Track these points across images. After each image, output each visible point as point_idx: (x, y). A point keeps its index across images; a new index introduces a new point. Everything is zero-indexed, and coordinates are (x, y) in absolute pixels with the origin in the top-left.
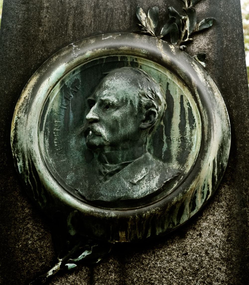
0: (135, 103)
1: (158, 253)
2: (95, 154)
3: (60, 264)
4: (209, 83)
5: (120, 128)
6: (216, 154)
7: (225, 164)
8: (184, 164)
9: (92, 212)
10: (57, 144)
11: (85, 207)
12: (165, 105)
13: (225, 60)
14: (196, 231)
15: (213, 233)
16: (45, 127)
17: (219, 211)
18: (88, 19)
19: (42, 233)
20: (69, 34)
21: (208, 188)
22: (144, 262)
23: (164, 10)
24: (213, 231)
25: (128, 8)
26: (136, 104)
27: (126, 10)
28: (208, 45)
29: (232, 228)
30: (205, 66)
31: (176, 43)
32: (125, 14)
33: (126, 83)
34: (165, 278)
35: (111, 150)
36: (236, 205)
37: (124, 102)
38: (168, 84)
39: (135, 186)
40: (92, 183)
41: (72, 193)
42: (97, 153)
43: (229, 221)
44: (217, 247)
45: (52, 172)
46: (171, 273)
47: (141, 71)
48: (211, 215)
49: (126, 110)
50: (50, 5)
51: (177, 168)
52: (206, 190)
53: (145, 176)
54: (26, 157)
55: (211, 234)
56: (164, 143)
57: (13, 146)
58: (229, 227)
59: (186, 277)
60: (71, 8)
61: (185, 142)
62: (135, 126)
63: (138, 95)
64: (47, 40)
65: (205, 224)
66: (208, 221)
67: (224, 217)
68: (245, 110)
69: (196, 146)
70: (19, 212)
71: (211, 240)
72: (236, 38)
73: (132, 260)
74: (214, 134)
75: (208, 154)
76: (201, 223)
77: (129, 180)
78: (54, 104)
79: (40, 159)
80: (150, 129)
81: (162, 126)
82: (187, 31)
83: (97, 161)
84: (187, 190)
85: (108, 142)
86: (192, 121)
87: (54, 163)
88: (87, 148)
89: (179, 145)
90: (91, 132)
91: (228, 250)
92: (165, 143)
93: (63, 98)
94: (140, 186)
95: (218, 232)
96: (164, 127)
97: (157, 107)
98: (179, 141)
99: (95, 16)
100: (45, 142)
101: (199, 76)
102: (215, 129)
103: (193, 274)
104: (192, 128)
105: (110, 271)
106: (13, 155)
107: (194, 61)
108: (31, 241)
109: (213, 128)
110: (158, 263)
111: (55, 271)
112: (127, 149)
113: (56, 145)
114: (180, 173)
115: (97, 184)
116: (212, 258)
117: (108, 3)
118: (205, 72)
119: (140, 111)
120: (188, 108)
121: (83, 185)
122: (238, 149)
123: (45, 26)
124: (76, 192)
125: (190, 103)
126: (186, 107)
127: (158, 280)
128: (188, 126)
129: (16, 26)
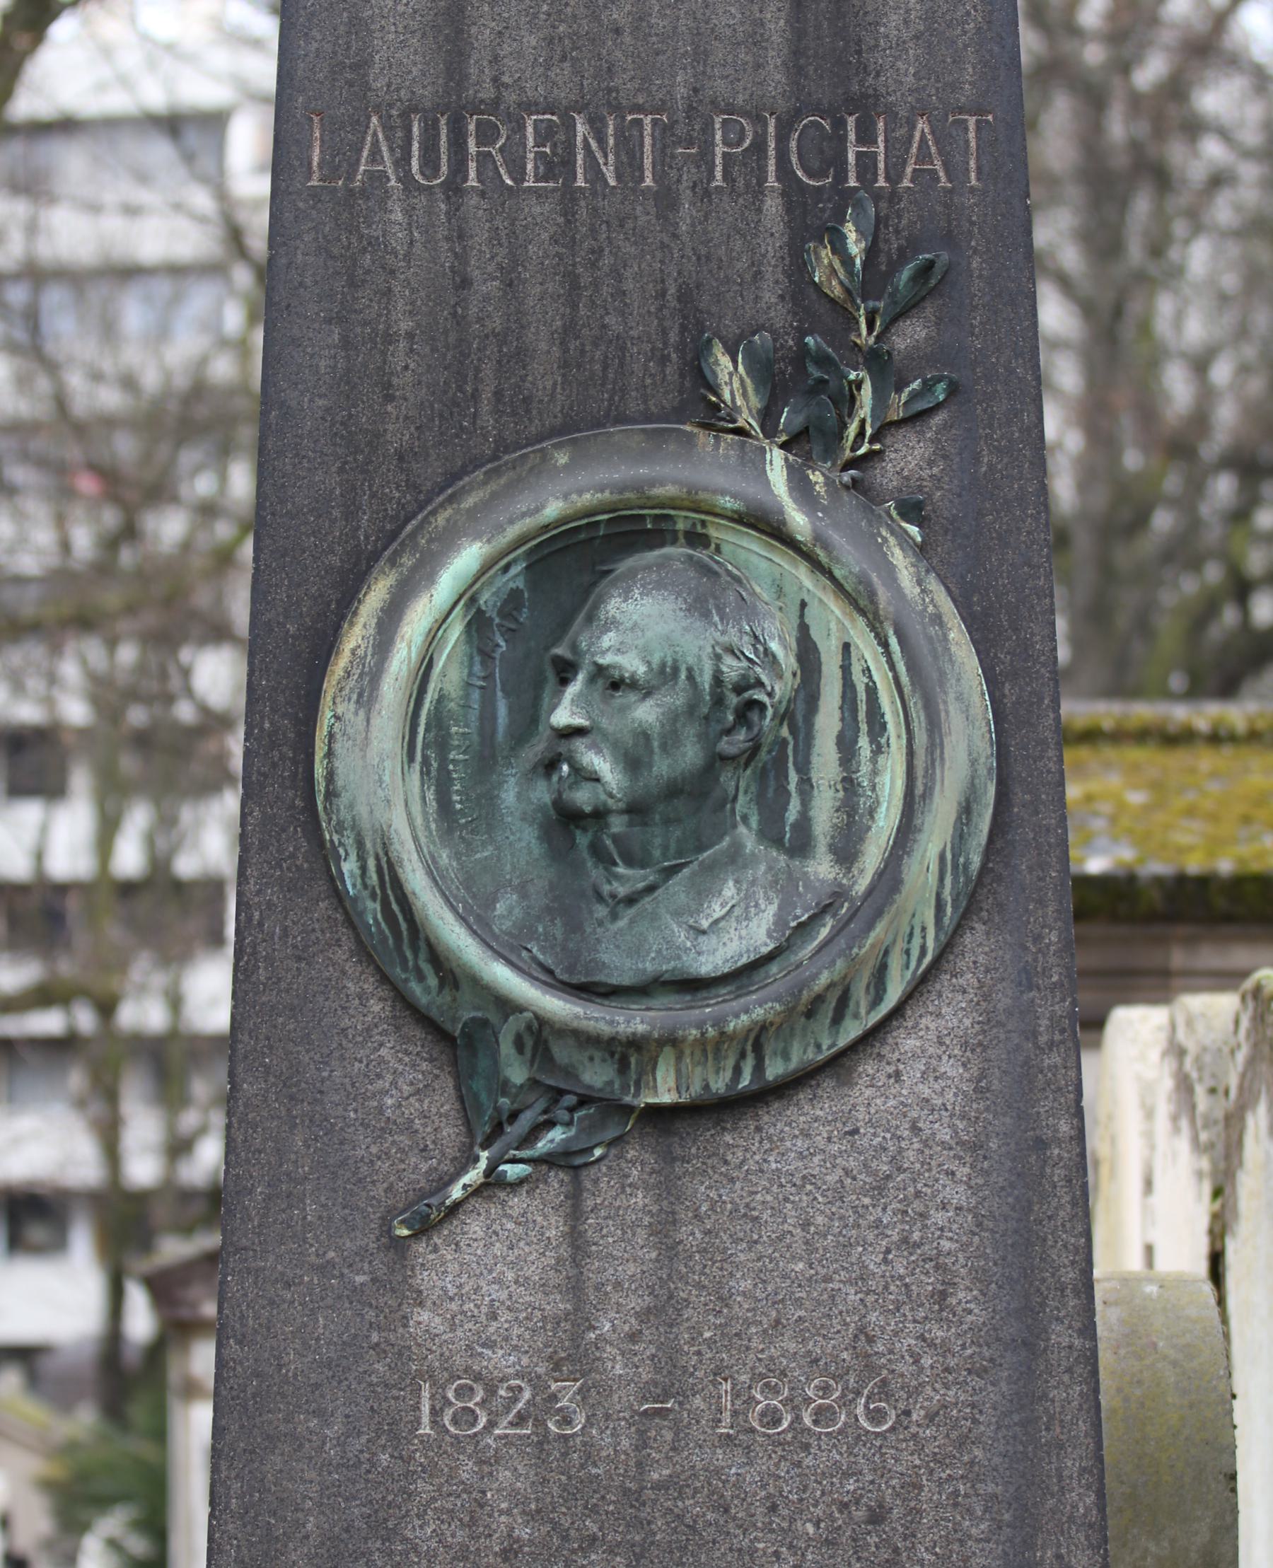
0: (701, 675)
1: (772, 1131)
2: (578, 833)
3: (483, 1164)
4: (932, 600)
5: (656, 758)
6: (951, 831)
7: (976, 860)
8: (852, 863)
9: (577, 1017)
10: (460, 802)
11: (556, 1006)
12: (794, 675)
13: (984, 516)
14: (884, 1063)
15: (935, 1070)
16: (423, 750)
17: (954, 1003)
18: (543, 377)
19: (423, 1073)
20: (482, 428)
21: (924, 937)
22: (729, 1157)
23: (791, 343)
24: (933, 1061)
25: (673, 337)
26: (706, 680)
27: (665, 344)
28: (931, 463)
29: (991, 1053)
30: (919, 539)
31: (829, 464)
32: (663, 356)
33: (674, 611)
34: (793, 1202)
35: (631, 824)
36: (1004, 984)
37: (667, 674)
38: (803, 605)
39: (705, 938)
40: (574, 927)
41: (514, 958)
42: (585, 830)
43: (984, 1032)
44: (946, 1110)
45: (451, 892)
46: (809, 1187)
47: (717, 562)
48: (931, 1014)
49: (676, 698)
50: (418, 325)
51: (831, 876)
52: (917, 942)
53: (733, 906)
54: (369, 845)
55: (930, 1073)
56: (789, 794)
57: (325, 808)
58: (984, 1051)
59: (854, 1197)
60: (487, 336)
61: (855, 794)
62: (703, 748)
63: (710, 650)
64: (412, 449)
65: (910, 1044)
66: (921, 1034)
67: (967, 1022)
68: (1043, 684)
69: (888, 809)
70: (351, 1011)
71: (927, 1091)
72: (1022, 442)
73: (693, 1151)
74: (943, 772)
75: (922, 837)
76: (900, 1041)
77: (684, 919)
78: (450, 674)
79: (415, 856)
80: (746, 755)
81: (784, 742)
82: (863, 422)
83: (585, 854)
84: (860, 948)
85: (620, 800)
86: (877, 728)
87: (455, 864)
88: (552, 812)
89: (838, 804)
90: (565, 768)
91: (977, 1118)
92: (794, 794)
93: (475, 653)
94: (718, 937)
95: (948, 1067)
96: (792, 743)
97: (769, 688)
98: (837, 791)
99: (565, 365)
100: (424, 798)
102: (946, 756)
103: (874, 1189)
104: (878, 751)
105: (630, 1185)
106: (328, 837)
107: (888, 525)
108: (392, 1096)
109: (942, 753)
110: (771, 1159)
111: (470, 1186)
112: (678, 820)
113: (458, 806)
114: (839, 894)
115: (588, 930)
116: (930, 1143)
117: (607, 320)
118: (919, 560)
119: (718, 701)
120: (867, 685)
121: (546, 933)
122: (1016, 810)
123: (406, 399)
124: (524, 953)
125: (872, 668)
126: (860, 681)
127: (772, 1208)
128: (864, 742)
129: (311, 401)
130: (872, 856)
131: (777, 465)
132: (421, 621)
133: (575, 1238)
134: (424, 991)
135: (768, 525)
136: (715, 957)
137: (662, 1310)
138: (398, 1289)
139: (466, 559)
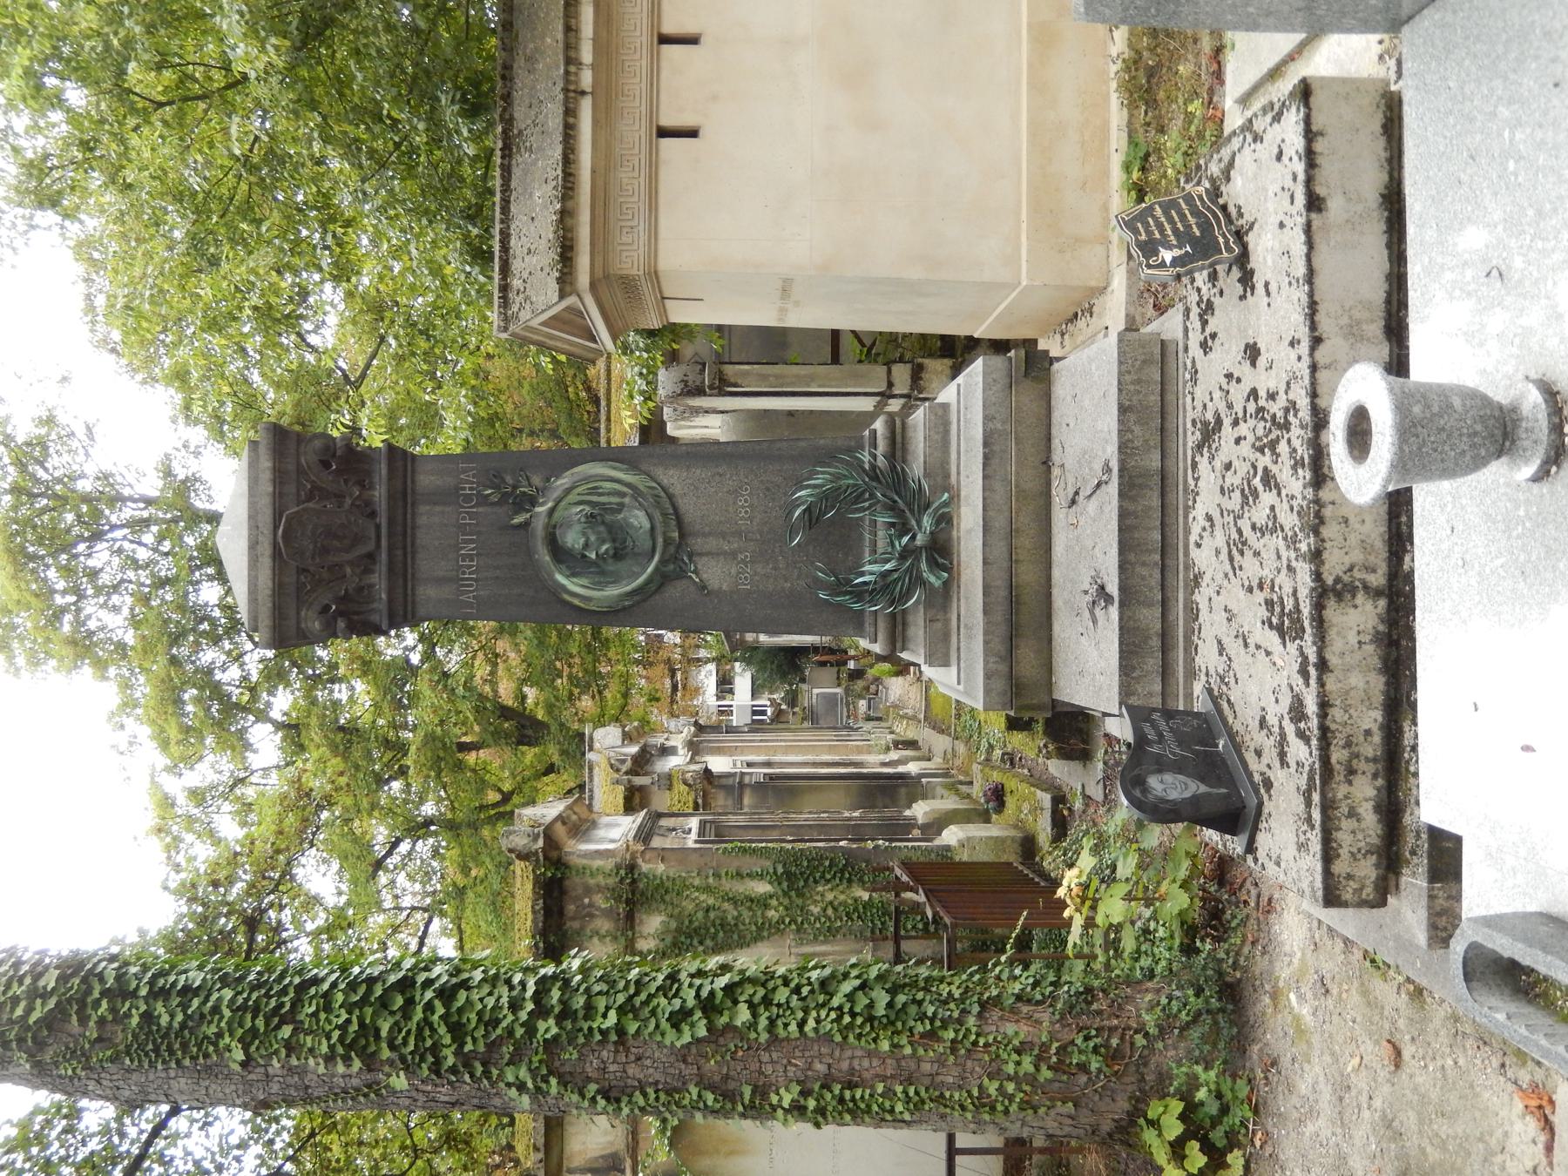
37: (584, 534)
101: (563, 482)
130: (625, 489)
131: (539, 509)
132: (574, 586)
133: (708, 554)
134: (653, 587)
135: (552, 511)
136: (647, 525)
137: (723, 535)
138: (718, 593)
139: (560, 578)
